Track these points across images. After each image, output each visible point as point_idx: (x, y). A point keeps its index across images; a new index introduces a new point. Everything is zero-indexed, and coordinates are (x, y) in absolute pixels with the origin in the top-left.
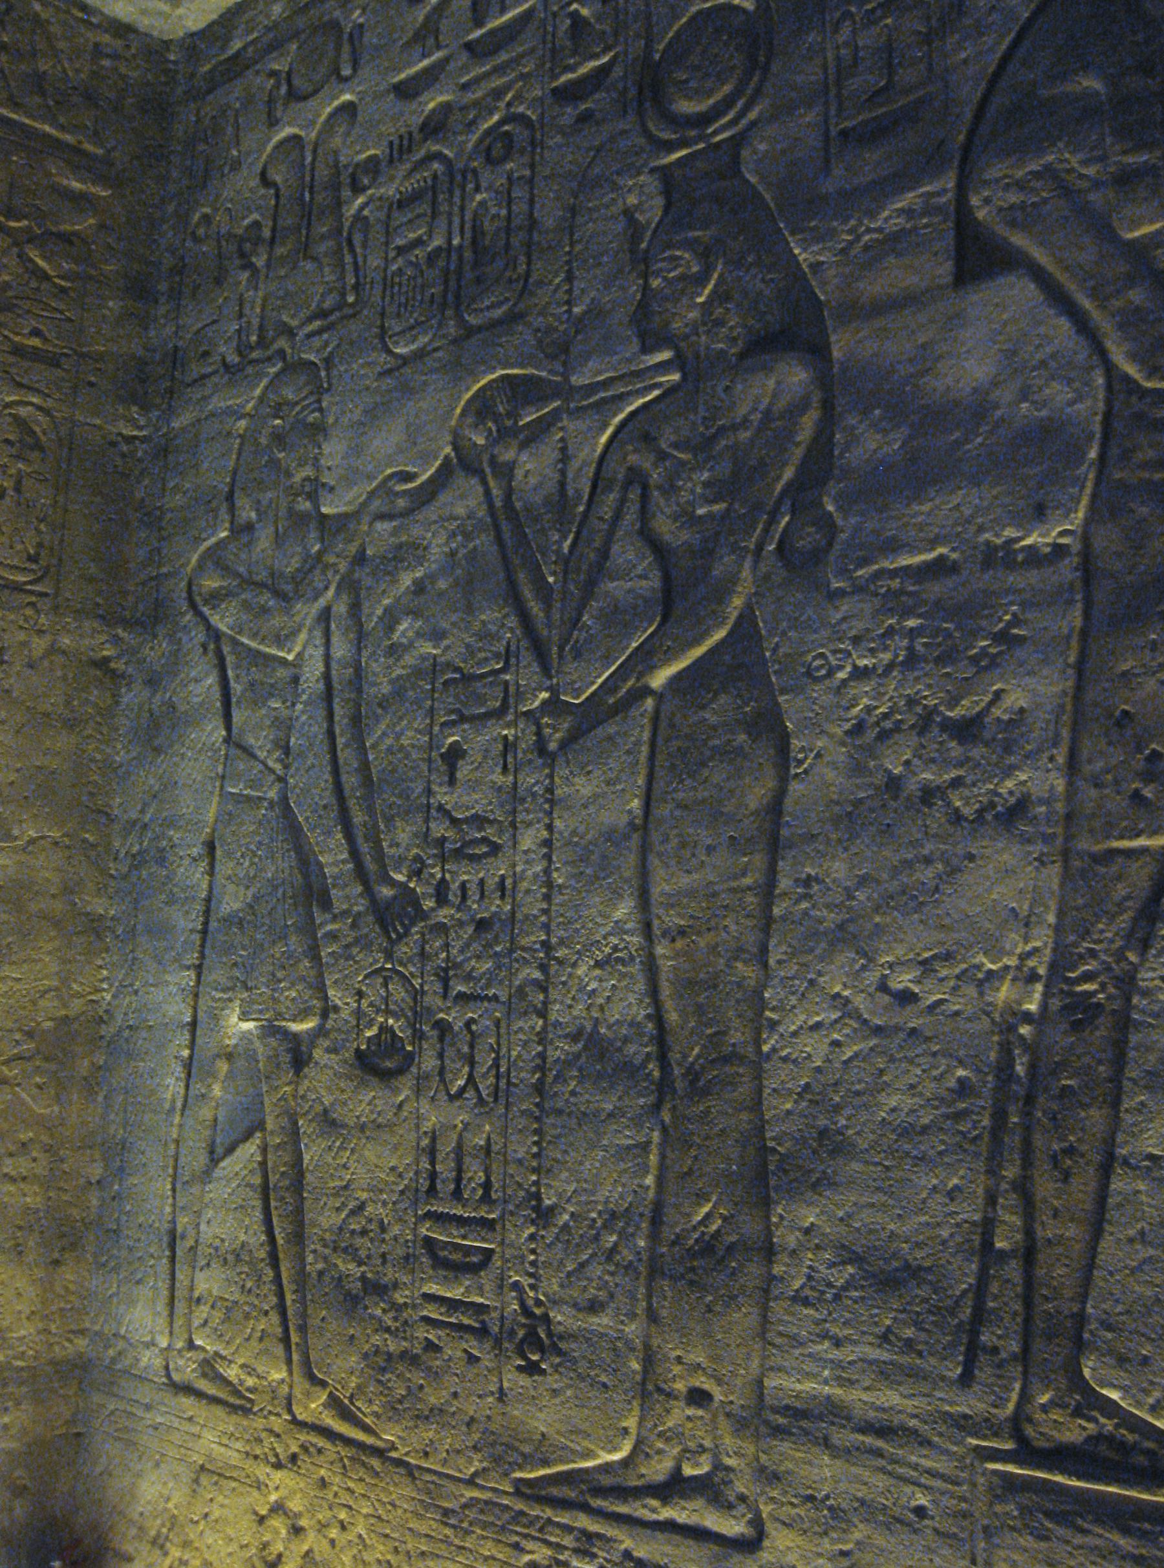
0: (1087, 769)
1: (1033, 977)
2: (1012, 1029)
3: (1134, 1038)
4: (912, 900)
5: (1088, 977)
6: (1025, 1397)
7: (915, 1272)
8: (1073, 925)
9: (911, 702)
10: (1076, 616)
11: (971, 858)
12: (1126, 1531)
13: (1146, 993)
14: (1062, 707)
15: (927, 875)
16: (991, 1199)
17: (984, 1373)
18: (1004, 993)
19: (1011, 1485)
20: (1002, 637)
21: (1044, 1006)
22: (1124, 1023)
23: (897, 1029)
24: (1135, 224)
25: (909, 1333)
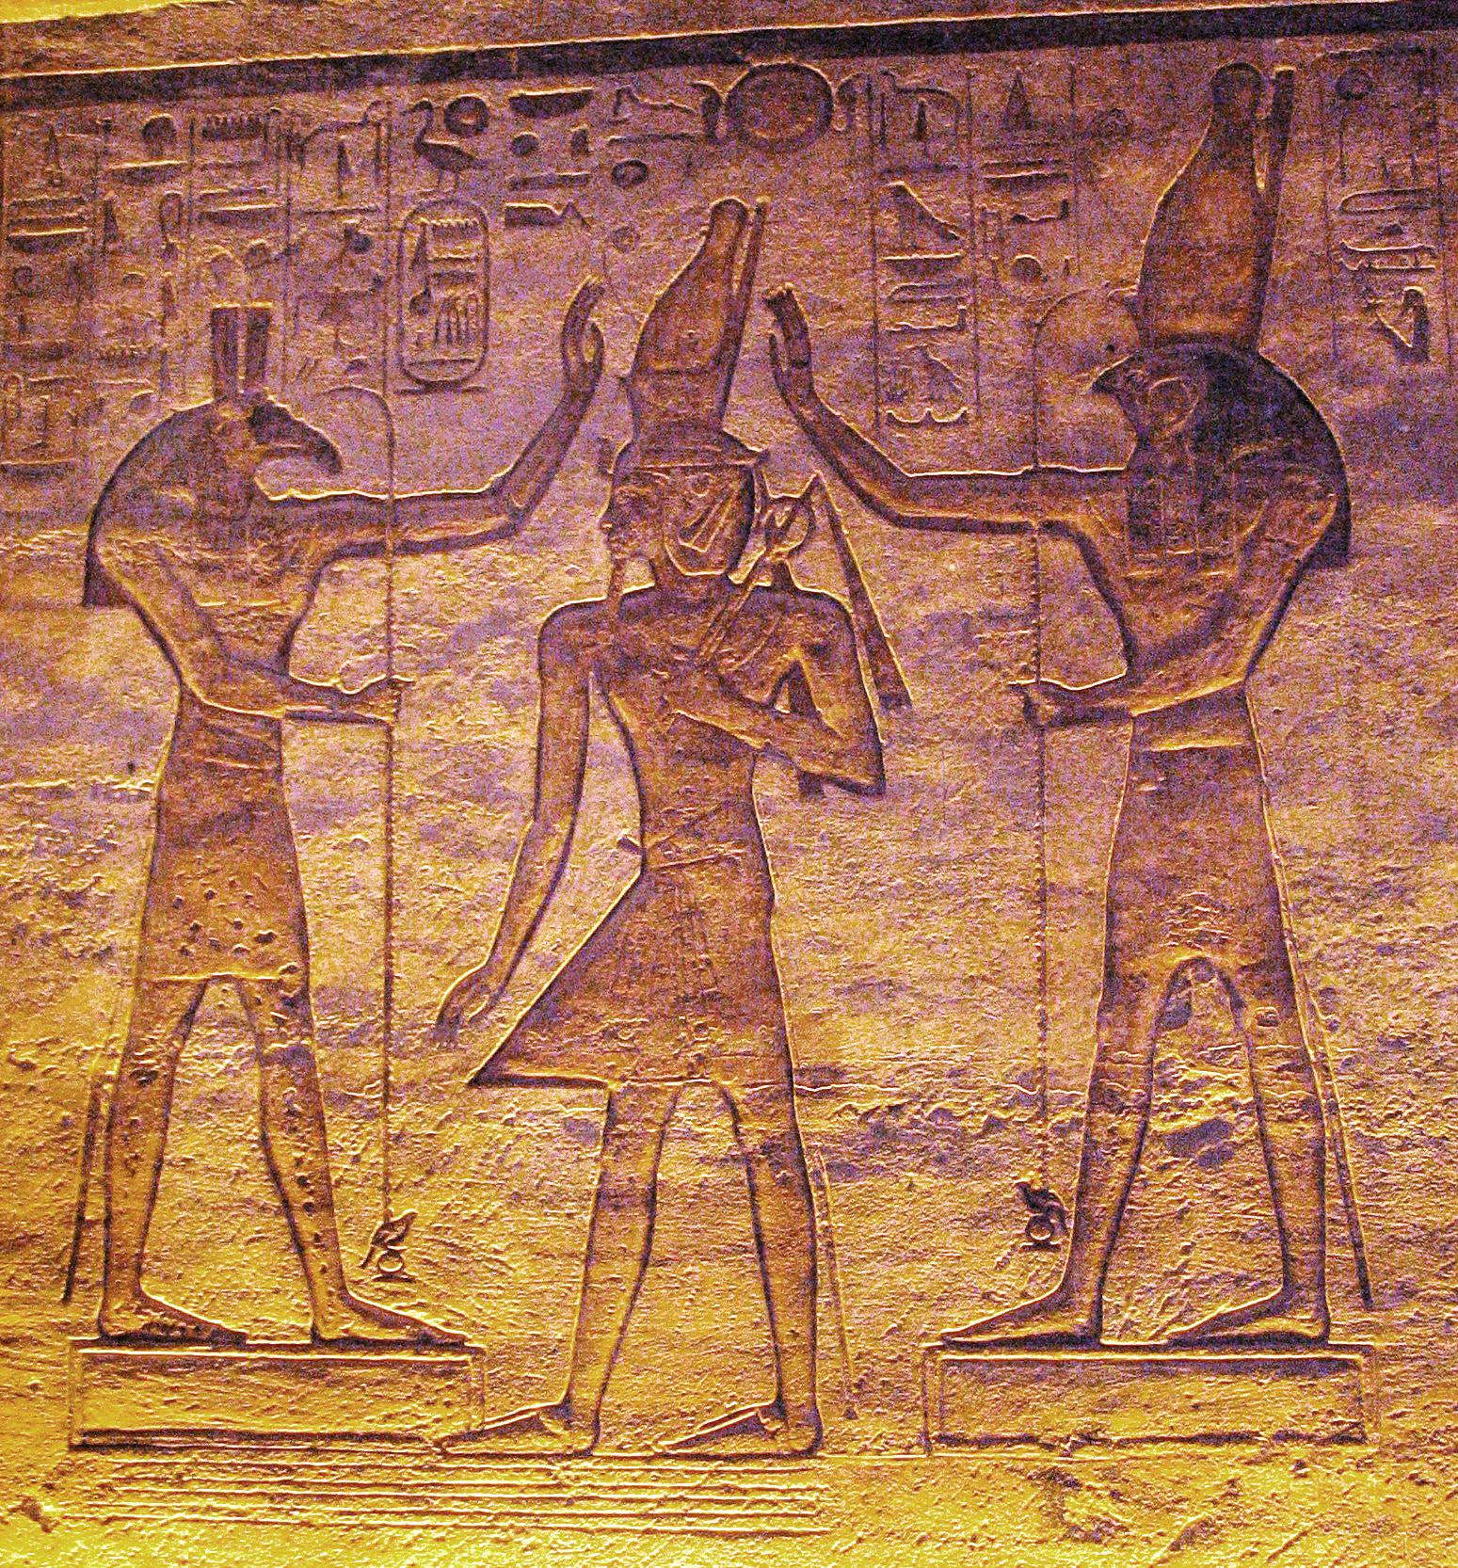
0: (154, 932)
1: (114, 1055)
2: (100, 1086)
3: (176, 1093)
4: (31, 1006)
5: (149, 1056)
6: (105, 1306)
7: (31, 1238)
8: (141, 1022)
9: (36, 877)
10: (152, 834)
11: (75, 980)
12: (167, 1375)
13: (184, 1065)
14: (139, 892)
15: (46, 990)
16: (84, 1190)
17: (78, 1295)
18: (93, 1064)
19: (95, 1360)
20: (99, 844)
21: (120, 1073)
22: (171, 1082)
23: (20, 1086)
24: (206, 598)
25: (26, 1277)
